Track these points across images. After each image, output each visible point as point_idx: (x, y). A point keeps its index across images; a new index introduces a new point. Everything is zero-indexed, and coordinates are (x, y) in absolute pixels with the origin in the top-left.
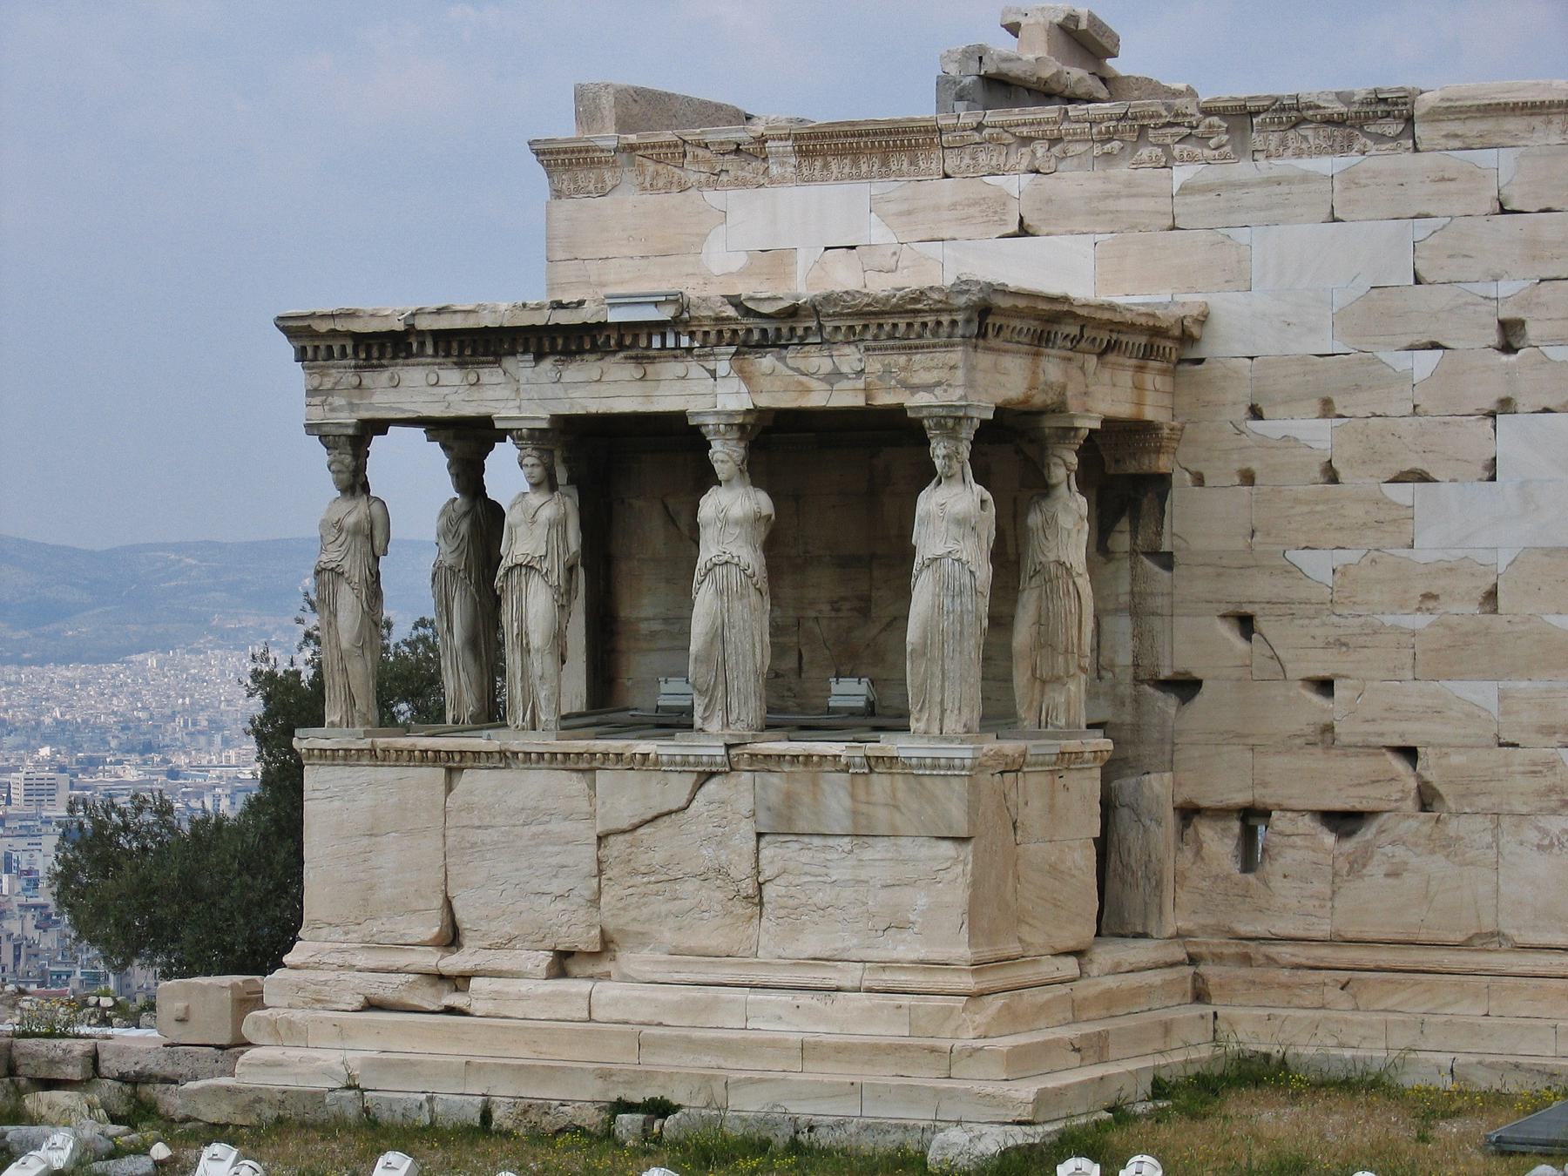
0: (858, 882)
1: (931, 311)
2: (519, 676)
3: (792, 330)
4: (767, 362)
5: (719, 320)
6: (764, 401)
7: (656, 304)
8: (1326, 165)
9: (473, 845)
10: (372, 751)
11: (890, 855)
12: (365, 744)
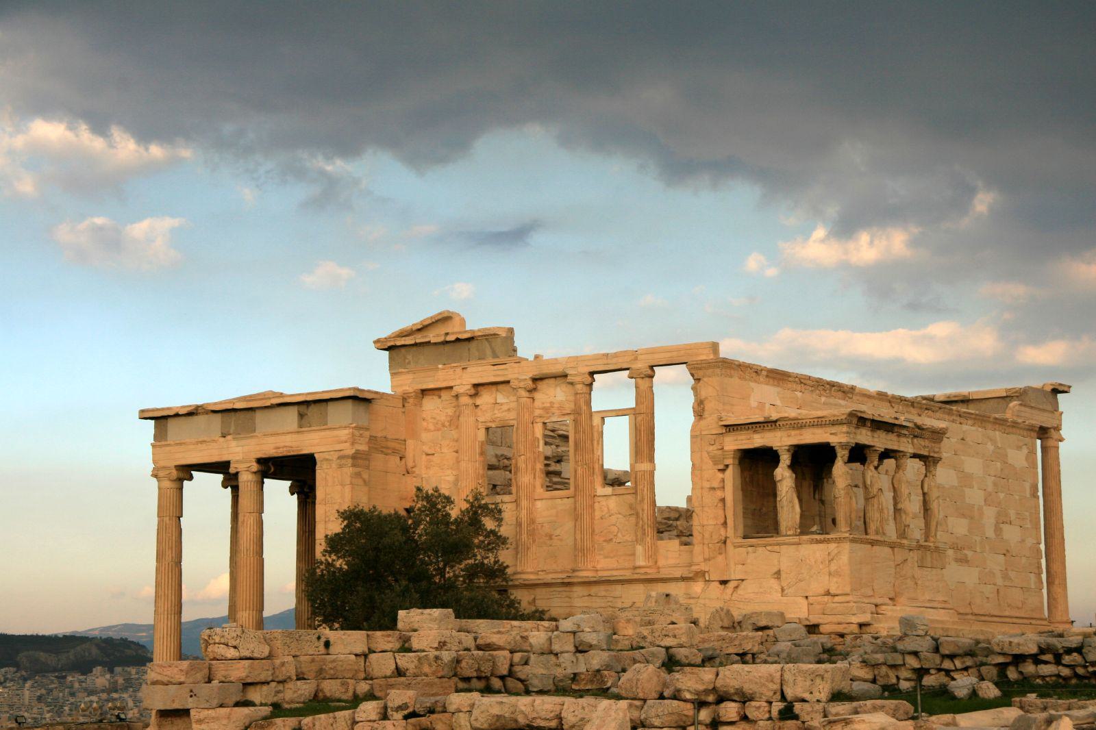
4: (915, 440)
5: (913, 428)
8: (842, 402)
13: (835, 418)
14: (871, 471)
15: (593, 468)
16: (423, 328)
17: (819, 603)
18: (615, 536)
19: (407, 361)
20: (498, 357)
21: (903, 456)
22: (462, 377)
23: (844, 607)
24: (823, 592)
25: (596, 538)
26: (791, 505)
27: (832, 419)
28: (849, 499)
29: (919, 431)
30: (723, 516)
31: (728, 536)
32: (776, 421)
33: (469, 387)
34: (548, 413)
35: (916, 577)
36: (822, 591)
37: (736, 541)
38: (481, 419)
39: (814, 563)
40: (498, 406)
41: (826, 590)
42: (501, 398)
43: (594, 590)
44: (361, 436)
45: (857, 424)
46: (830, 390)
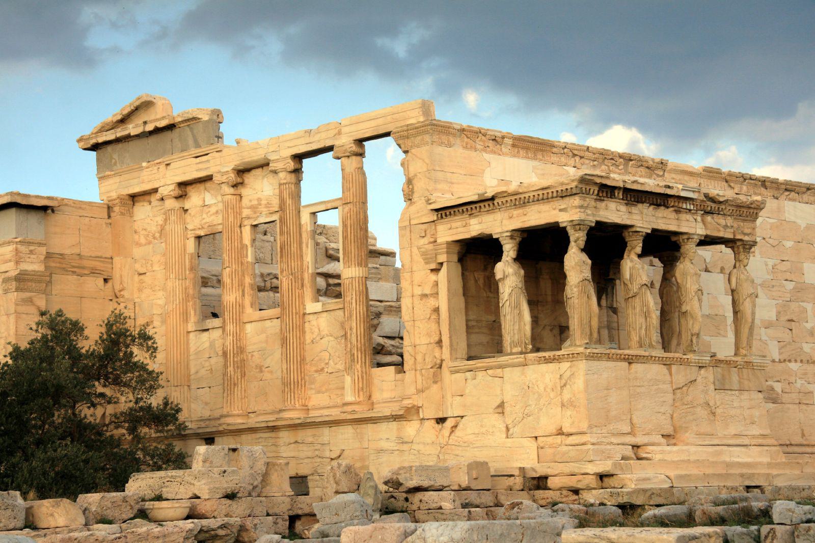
0: (741, 407)
1: (755, 208)
2: (644, 327)
3: (719, 208)
4: (709, 218)
5: (703, 201)
6: (709, 233)
7: (693, 191)
9: (638, 393)
10: (609, 354)
11: (748, 397)
12: (608, 351)
13: (564, 188)
14: (632, 261)
15: (302, 280)
16: (123, 121)
17: (551, 446)
18: (327, 364)
19: (113, 161)
20: (200, 147)
21: (688, 239)
22: (164, 175)
23: (577, 450)
24: (554, 431)
25: (308, 367)
26: (516, 311)
27: (559, 189)
28: (585, 298)
29: (711, 206)
30: (438, 333)
31: (444, 357)
32: (493, 199)
33: (172, 187)
34: (255, 213)
35: (711, 404)
36: (552, 429)
37: (456, 364)
38: (190, 227)
39: (543, 391)
40: (206, 208)
41: (559, 428)
42: (209, 199)
43: (302, 435)
44: (31, 252)
45: (598, 195)
46: (626, 165)
